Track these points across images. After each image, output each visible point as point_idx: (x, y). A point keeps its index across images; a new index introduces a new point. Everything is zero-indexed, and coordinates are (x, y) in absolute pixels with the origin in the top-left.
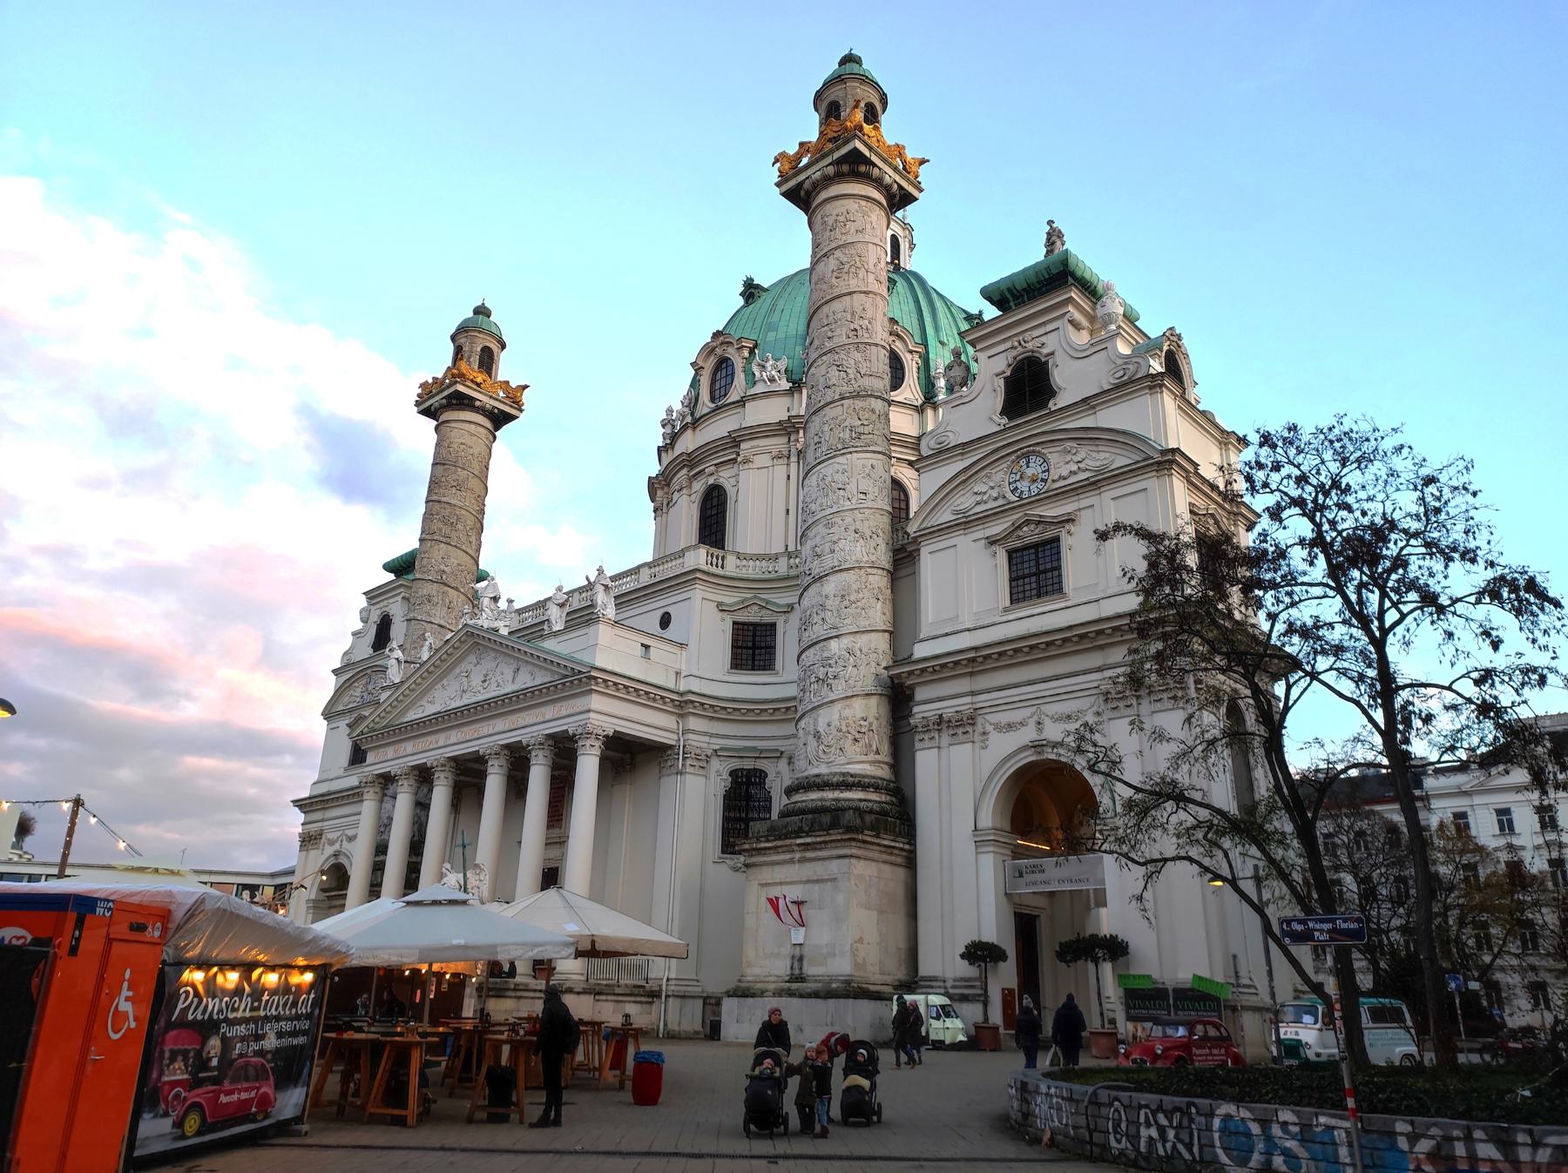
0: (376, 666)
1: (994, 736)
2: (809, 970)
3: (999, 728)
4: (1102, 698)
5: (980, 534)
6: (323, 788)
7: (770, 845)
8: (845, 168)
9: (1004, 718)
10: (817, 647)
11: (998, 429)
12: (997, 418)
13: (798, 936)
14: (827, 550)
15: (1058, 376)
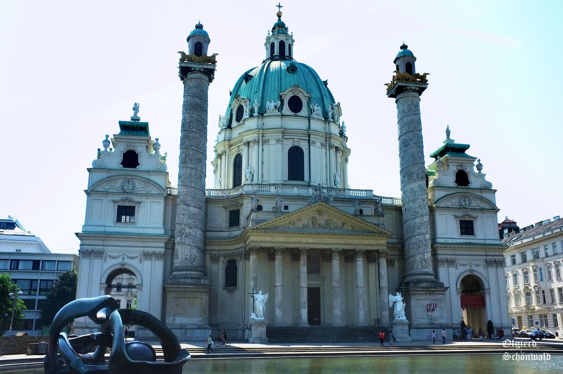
0: (135, 176)
1: (459, 266)
2: (433, 322)
3: (460, 265)
4: (485, 263)
5: (452, 213)
6: (101, 229)
7: (421, 289)
8: (420, 90)
9: (462, 262)
10: (423, 235)
11: (455, 186)
12: (454, 183)
13: (429, 313)
14: (424, 208)
15: (471, 178)
